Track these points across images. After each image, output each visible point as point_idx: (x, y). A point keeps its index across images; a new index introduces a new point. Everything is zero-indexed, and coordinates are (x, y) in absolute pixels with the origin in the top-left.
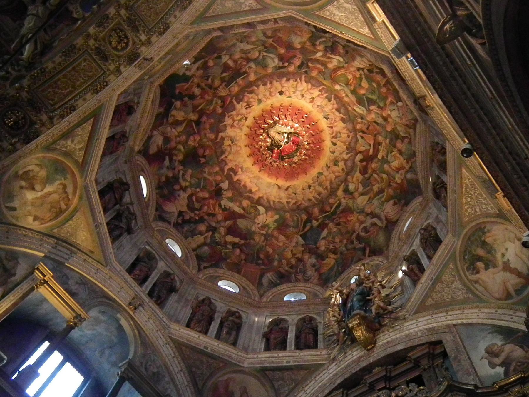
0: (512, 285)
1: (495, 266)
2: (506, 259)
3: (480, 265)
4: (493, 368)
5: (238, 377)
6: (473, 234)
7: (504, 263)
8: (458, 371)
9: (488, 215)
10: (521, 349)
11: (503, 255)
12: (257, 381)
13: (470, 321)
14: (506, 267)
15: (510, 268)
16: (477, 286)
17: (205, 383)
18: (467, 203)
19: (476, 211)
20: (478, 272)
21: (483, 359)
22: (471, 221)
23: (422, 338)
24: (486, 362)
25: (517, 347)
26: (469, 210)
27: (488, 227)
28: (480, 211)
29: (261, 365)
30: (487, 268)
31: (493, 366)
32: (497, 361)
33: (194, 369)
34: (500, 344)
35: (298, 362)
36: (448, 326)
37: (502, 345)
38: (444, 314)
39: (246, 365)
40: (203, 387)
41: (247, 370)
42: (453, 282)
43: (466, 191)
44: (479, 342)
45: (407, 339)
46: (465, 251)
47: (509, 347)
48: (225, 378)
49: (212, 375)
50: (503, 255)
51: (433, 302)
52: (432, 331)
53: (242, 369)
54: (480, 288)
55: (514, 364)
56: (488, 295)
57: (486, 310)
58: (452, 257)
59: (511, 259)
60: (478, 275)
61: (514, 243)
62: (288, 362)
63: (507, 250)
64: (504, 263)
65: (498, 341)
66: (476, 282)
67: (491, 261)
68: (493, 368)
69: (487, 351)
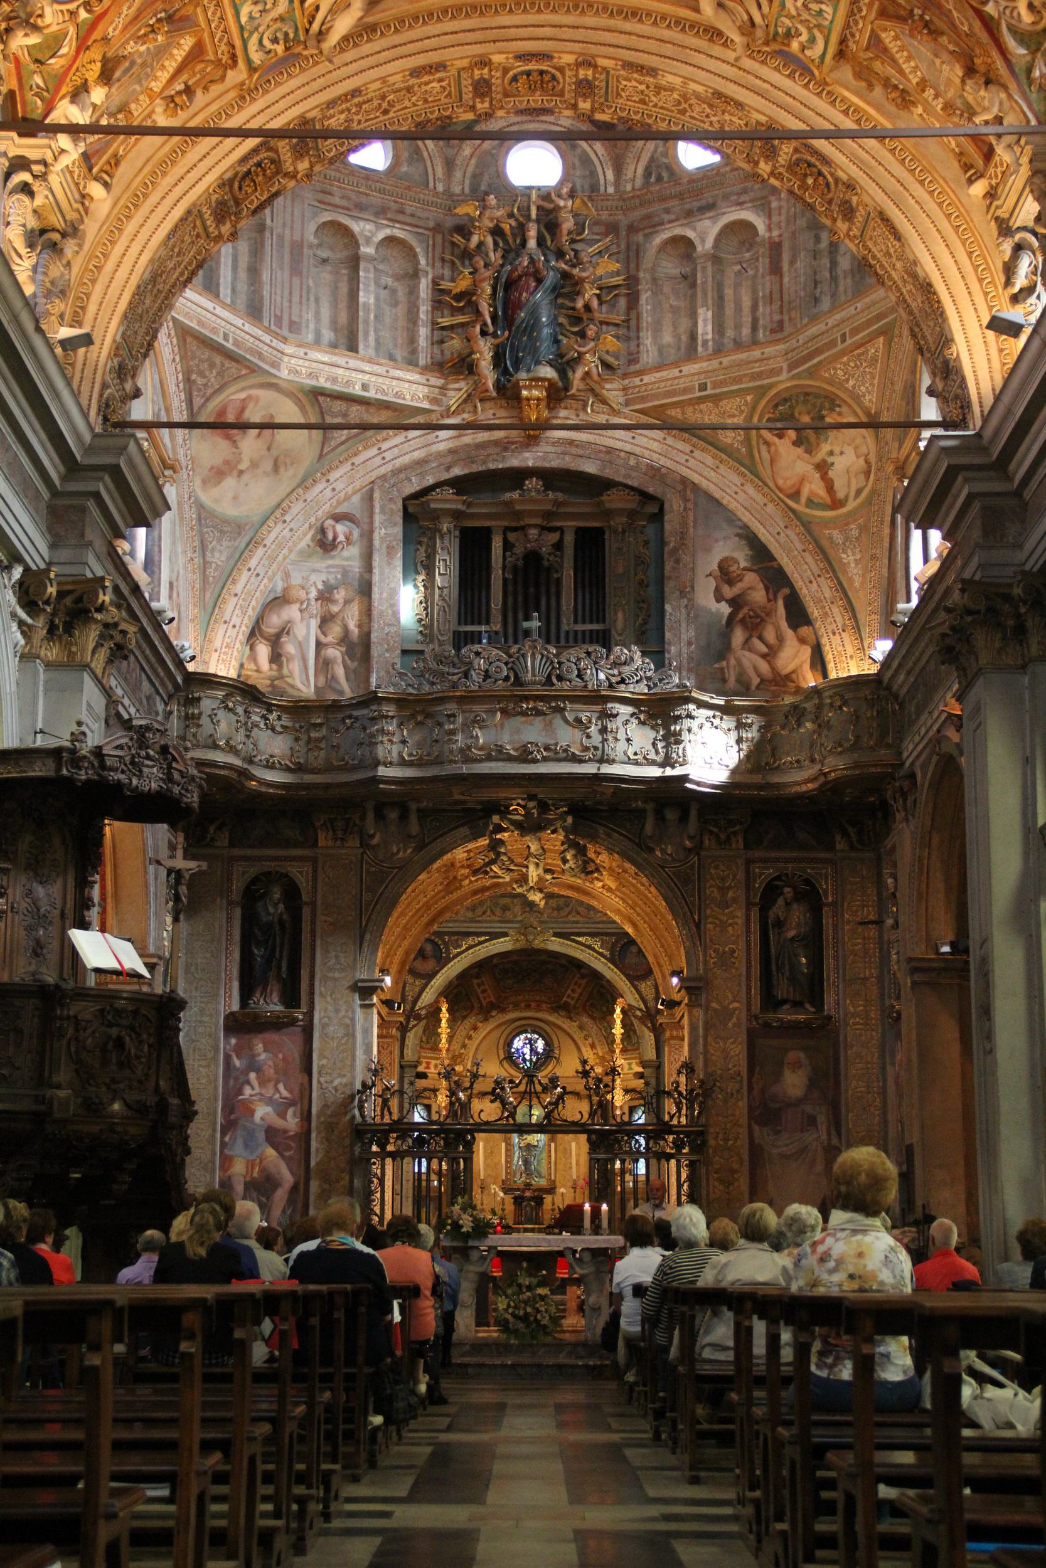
0: (811, 492)
1: (809, 452)
2: (830, 460)
3: (792, 434)
4: (718, 601)
5: (265, 395)
6: (817, 396)
7: (824, 461)
8: (670, 578)
9: (857, 398)
10: (763, 592)
11: (831, 453)
12: (296, 409)
13: (717, 494)
14: (823, 468)
15: (826, 473)
16: (764, 448)
17: (204, 405)
18: (845, 364)
19: (847, 381)
20: (780, 437)
21: (711, 579)
22: (830, 382)
23: (634, 474)
24: (712, 583)
25: (761, 585)
26: (840, 372)
27: (844, 409)
28: (854, 387)
29: (314, 383)
30: (797, 443)
31: (718, 600)
32: (728, 592)
33: (194, 377)
34: (743, 564)
35: (383, 392)
36: (684, 481)
37: (745, 569)
38: (687, 448)
39: (284, 374)
40: (200, 408)
41: (283, 384)
42: (734, 416)
43: (859, 355)
44: (717, 541)
45: (607, 457)
46: (785, 400)
47: (751, 578)
48: (243, 395)
49: (221, 389)
50: (831, 453)
51: (680, 416)
52: (655, 472)
53: (274, 381)
54: (766, 455)
55: (745, 610)
56: (769, 471)
57: (751, 490)
58: (761, 391)
59: (836, 466)
60: (776, 440)
61: (858, 457)
62: (365, 387)
63: (842, 453)
64: (824, 461)
65: (742, 557)
66: (767, 443)
67: (808, 441)
68: (718, 601)
69: (720, 567)
